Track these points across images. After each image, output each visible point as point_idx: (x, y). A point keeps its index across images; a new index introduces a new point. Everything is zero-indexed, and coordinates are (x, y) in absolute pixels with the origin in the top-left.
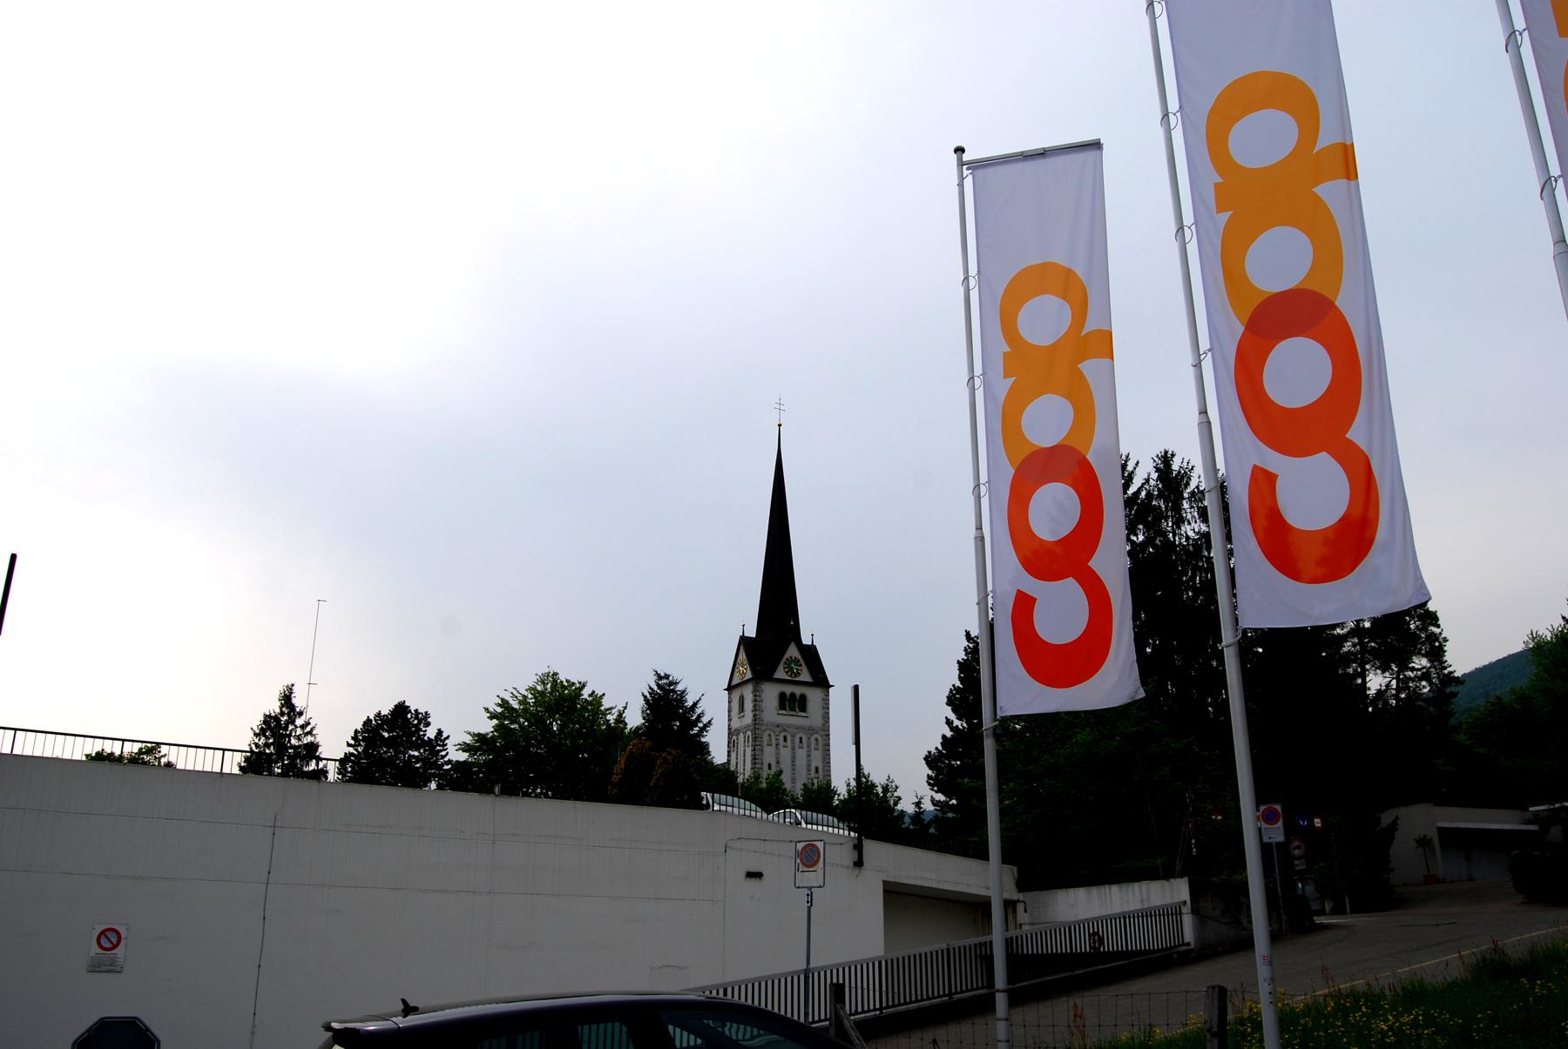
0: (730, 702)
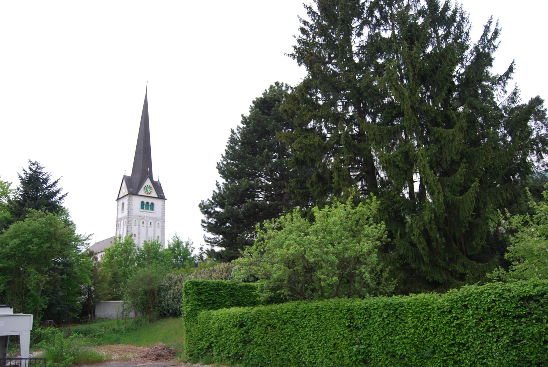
0: (118, 206)
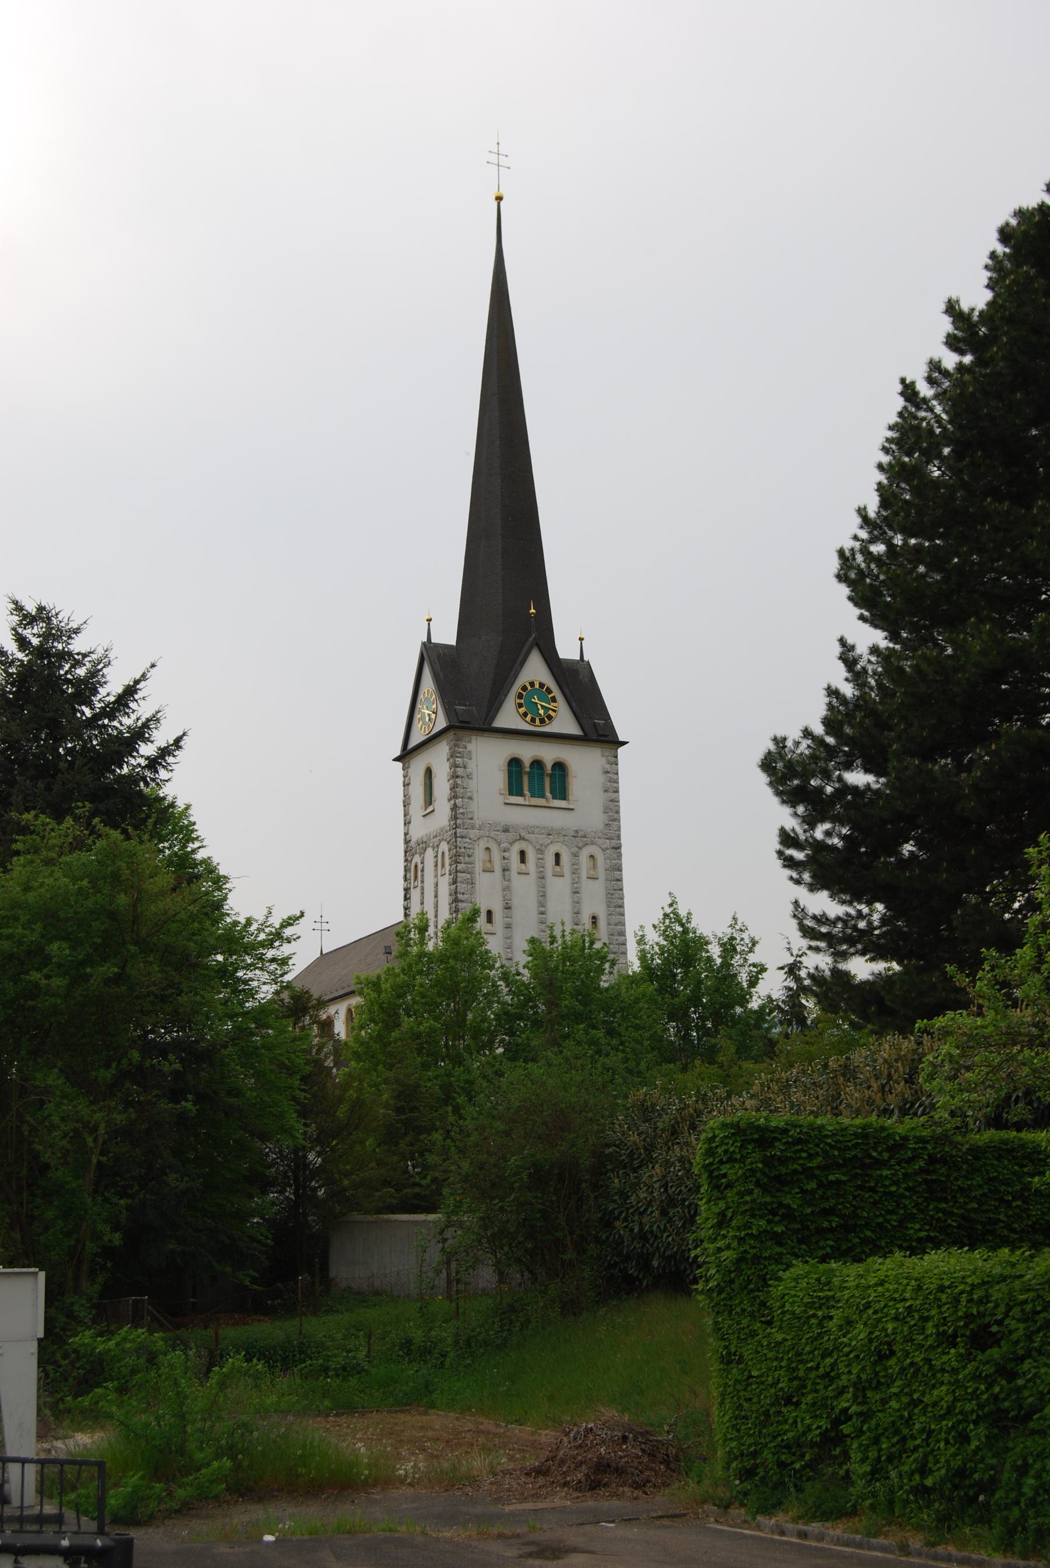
0: (406, 785)
